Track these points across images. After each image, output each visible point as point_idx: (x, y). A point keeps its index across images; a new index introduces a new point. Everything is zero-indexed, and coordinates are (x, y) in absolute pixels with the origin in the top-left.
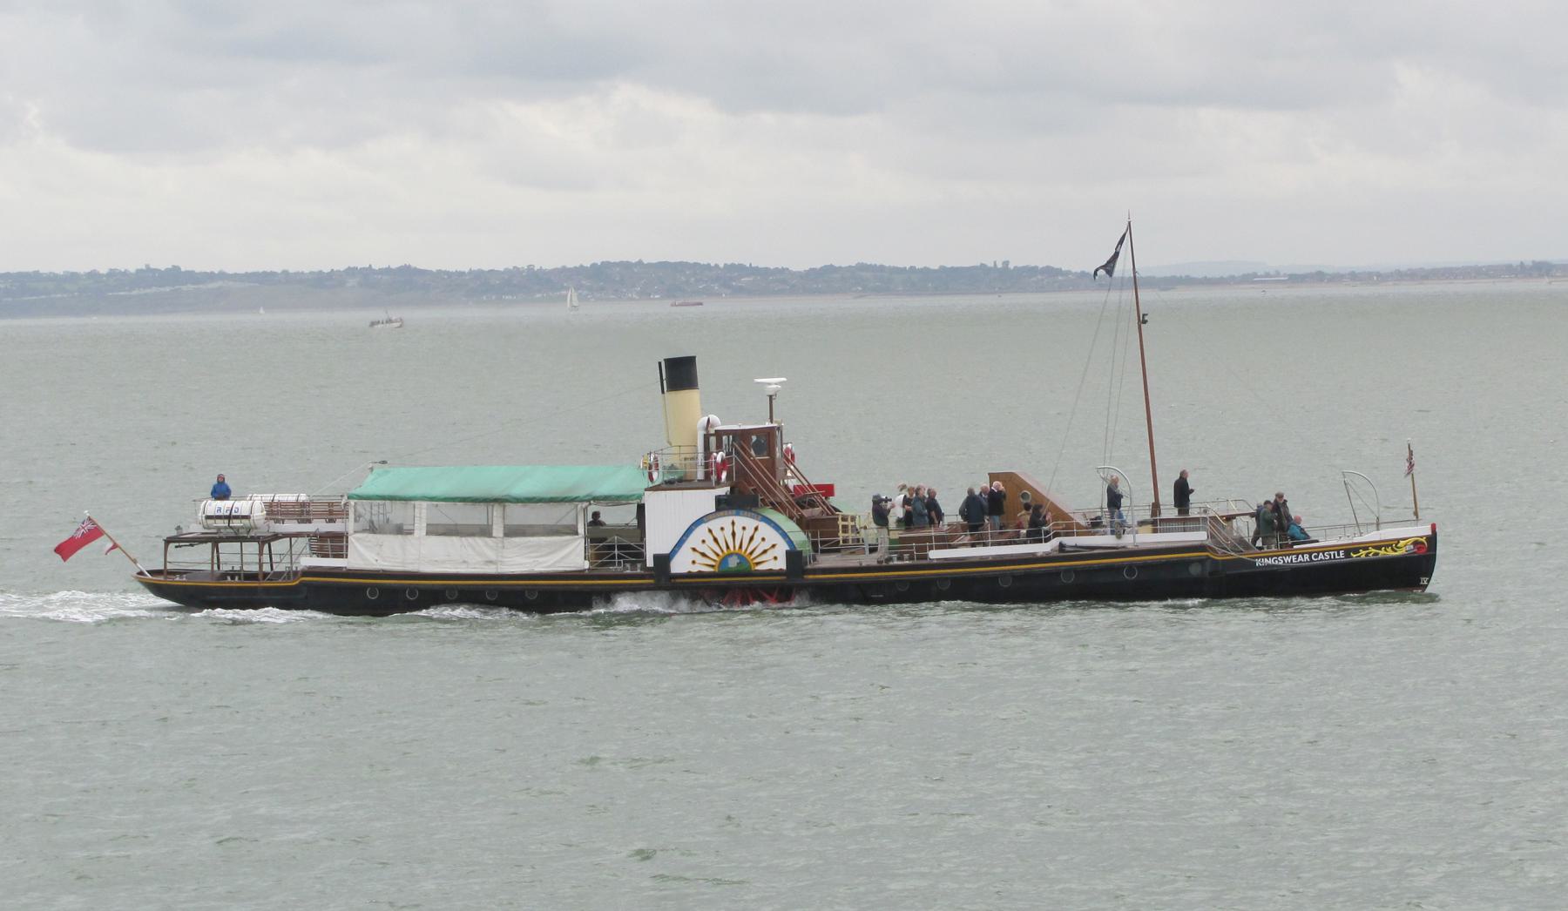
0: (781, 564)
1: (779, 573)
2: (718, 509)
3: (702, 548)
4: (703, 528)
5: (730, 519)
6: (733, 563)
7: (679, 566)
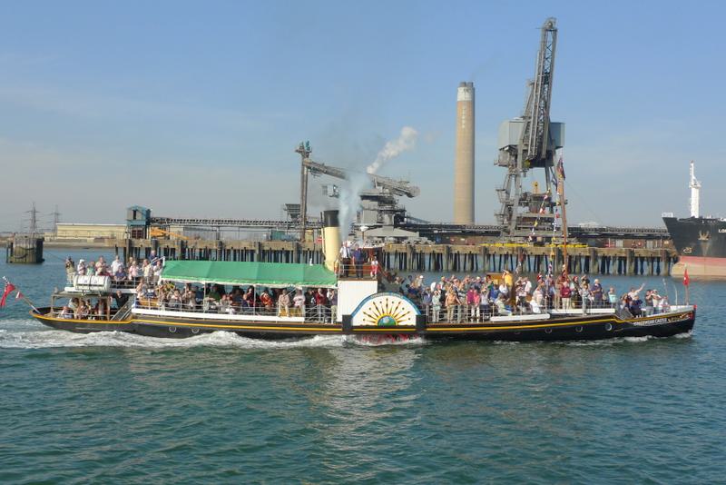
0: (413, 322)
1: (412, 327)
2: (378, 292)
3: (390, 303)
4: (371, 301)
5: (386, 297)
6: (385, 321)
7: (357, 322)
